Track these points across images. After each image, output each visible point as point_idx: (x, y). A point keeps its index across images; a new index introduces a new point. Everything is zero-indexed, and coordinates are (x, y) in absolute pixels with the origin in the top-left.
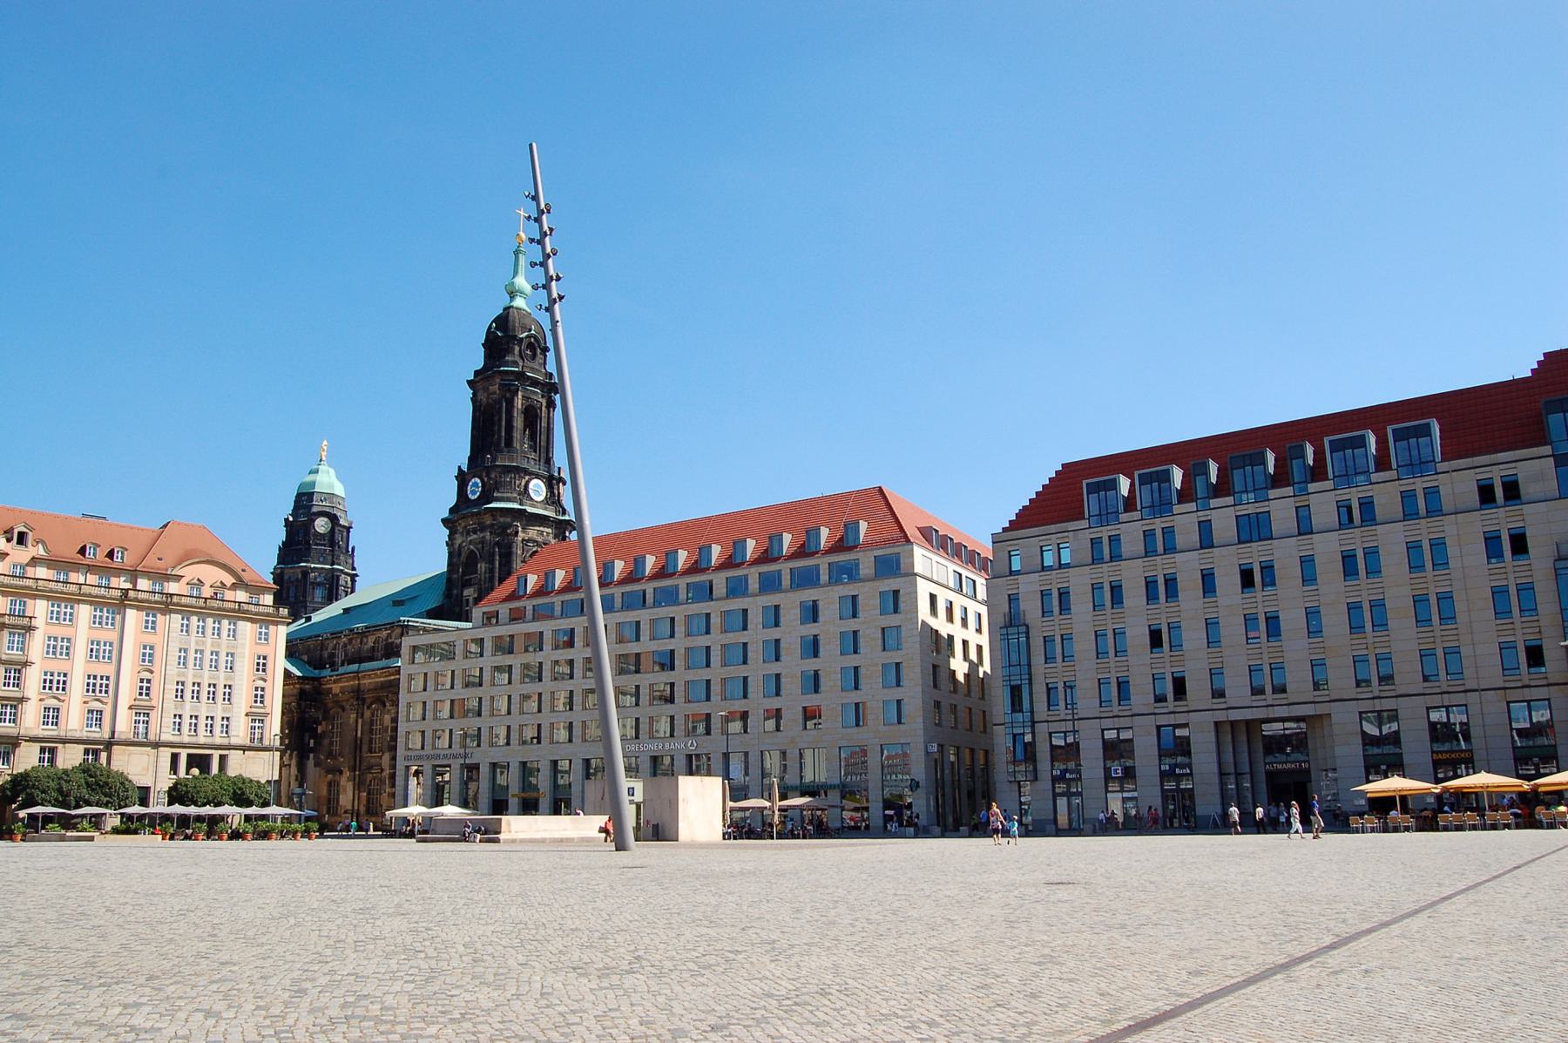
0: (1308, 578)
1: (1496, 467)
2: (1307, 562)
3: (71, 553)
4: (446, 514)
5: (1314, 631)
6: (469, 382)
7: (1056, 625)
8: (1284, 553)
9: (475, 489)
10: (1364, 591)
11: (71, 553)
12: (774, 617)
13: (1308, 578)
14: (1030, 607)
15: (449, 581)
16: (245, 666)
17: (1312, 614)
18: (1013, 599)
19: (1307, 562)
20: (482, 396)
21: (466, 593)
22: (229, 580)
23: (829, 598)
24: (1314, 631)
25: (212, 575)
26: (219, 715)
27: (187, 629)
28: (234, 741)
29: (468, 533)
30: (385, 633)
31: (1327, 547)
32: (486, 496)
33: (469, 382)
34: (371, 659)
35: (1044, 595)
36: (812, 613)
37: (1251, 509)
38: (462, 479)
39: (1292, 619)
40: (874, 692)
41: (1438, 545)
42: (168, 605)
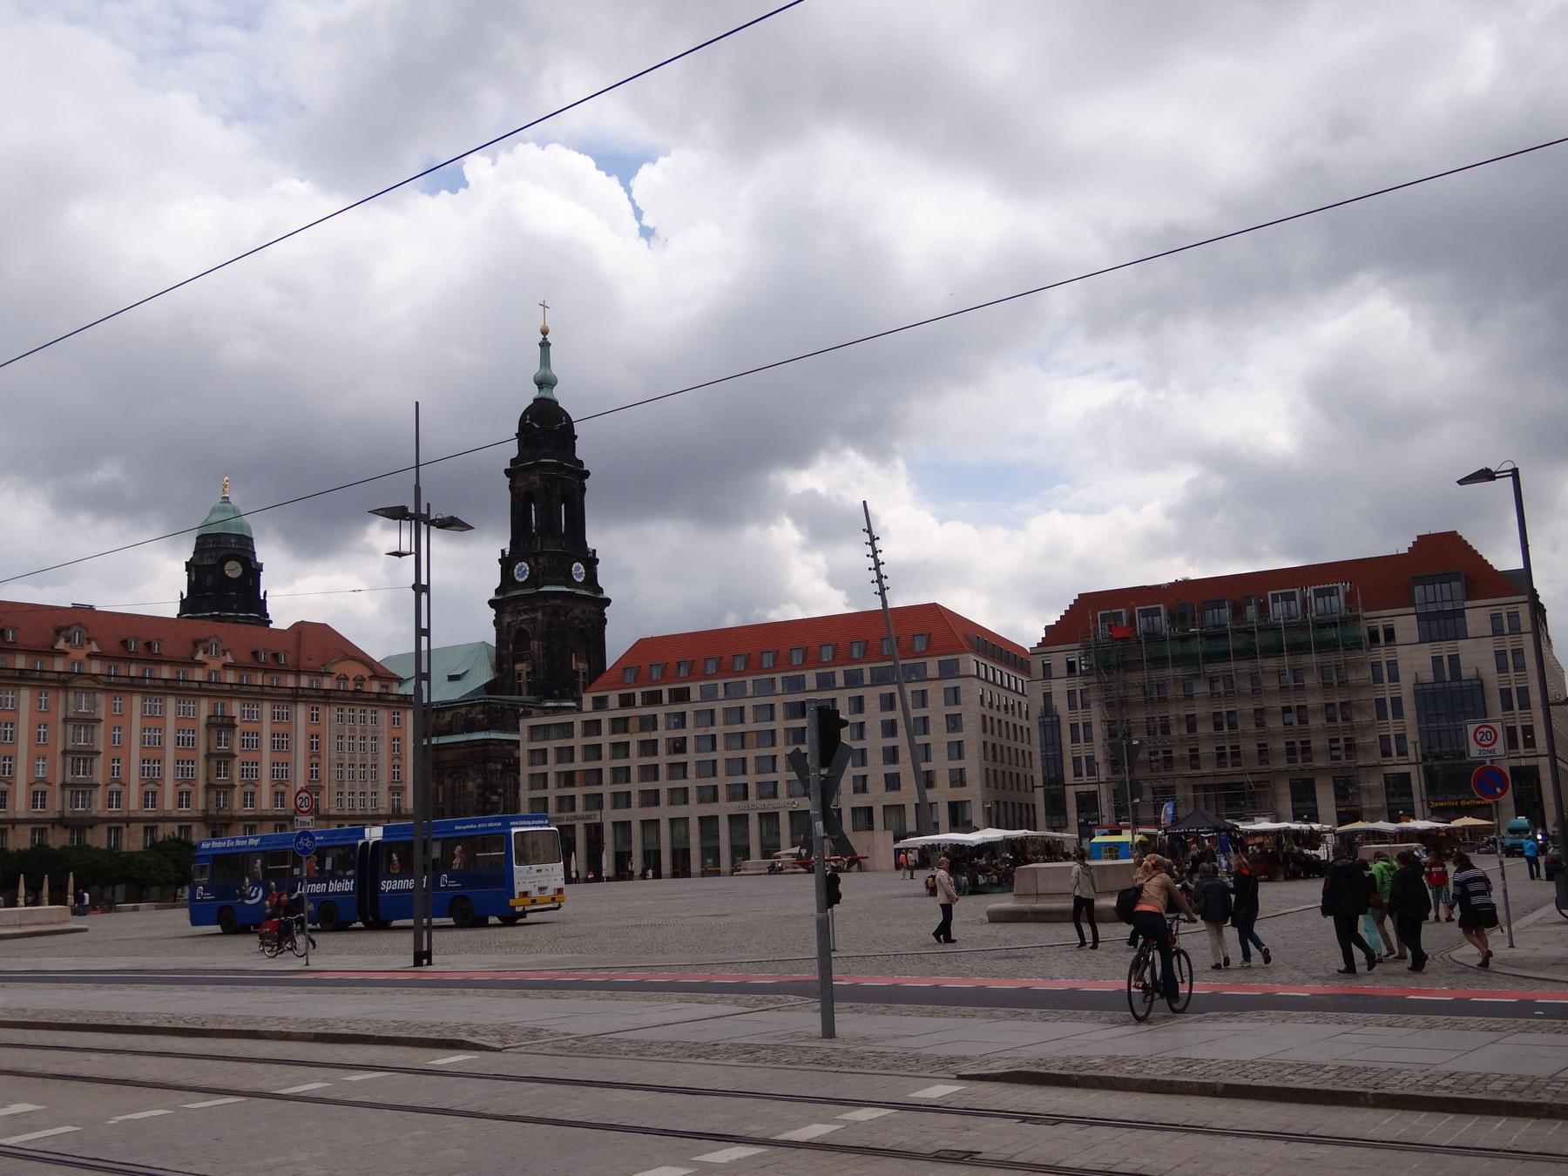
3: (245, 658)
4: (492, 595)
6: (507, 471)
9: (522, 571)
11: (245, 658)
14: (1061, 703)
15: (498, 655)
16: (384, 748)
18: (1047, 696)
20: (519, 484)
21: (518, 667)
22: (366, 673)
25: (352, 670)
26: (369, 790)
27: (341, 719)
28: (381, 812)
29: (519, 613)
30: (463, 711)
32: (533, 580)
33: (507, 471)
34: (450, 733)
38: (507, 563)
42: (327, 697)
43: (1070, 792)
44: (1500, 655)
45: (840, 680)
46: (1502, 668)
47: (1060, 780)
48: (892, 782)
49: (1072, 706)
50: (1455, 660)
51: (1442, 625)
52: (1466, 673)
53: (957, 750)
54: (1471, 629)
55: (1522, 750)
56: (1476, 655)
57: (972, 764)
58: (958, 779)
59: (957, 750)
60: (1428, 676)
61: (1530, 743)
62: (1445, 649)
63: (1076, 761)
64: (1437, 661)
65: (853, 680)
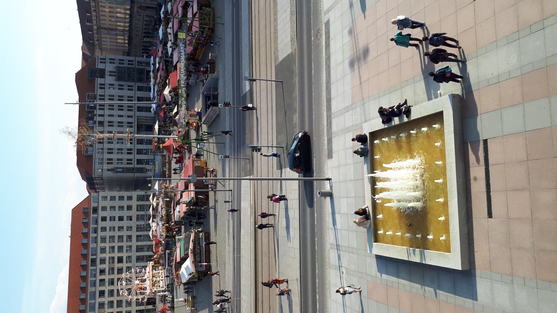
0: (112, 116)
1: (97, 86)
2: (109, 116)
5: (121, 116)
7: (115, 162)
8: (107, 119)
10: (116, 107)
12: (104, 229)
13: (112, 116)
14: (110, 167)
17: (119, 116)
18: (108, 170)
19: (109, 116)
23: (101, 214)
24: (121, 116)
31: (107, 112)
35: (108, 163)
36: (104, 219)
37: (97, 124)
39: (120, 119)
40: (125, 203)
41: (110, 96)
43: (136, 166)
44: (110, 63)
45: (95, 235)
46: (114, 63)
47: (133, 169)
48: (130, 218)
49: (112, 163)
50: (110, 72)
51: (102, 73)
52: (114, 70)
53: (121, 198)
54: (103, 67)
55: (134, 63)
56: (109, 68)
57: (126, 194)
58: (130, 198)
59: (121, 198)
60: (114, 78)
61: (132, 61)
62: (107, 73)
63: (128, 163)
64: (110, 75)
65: (96, 231)
